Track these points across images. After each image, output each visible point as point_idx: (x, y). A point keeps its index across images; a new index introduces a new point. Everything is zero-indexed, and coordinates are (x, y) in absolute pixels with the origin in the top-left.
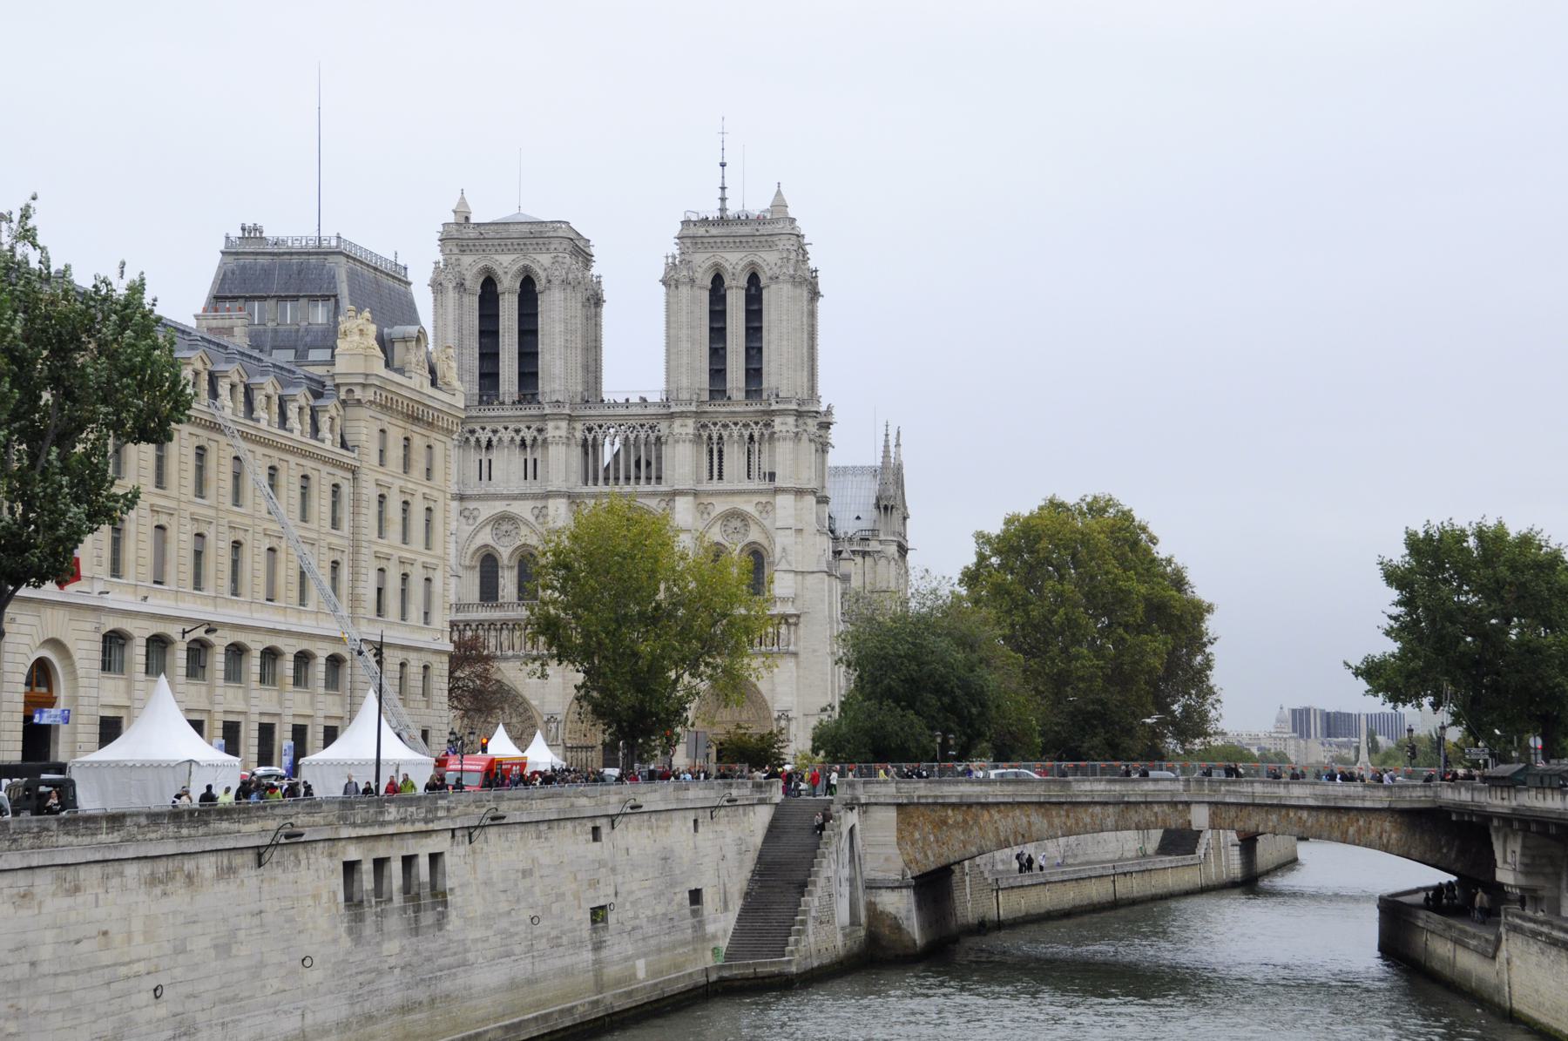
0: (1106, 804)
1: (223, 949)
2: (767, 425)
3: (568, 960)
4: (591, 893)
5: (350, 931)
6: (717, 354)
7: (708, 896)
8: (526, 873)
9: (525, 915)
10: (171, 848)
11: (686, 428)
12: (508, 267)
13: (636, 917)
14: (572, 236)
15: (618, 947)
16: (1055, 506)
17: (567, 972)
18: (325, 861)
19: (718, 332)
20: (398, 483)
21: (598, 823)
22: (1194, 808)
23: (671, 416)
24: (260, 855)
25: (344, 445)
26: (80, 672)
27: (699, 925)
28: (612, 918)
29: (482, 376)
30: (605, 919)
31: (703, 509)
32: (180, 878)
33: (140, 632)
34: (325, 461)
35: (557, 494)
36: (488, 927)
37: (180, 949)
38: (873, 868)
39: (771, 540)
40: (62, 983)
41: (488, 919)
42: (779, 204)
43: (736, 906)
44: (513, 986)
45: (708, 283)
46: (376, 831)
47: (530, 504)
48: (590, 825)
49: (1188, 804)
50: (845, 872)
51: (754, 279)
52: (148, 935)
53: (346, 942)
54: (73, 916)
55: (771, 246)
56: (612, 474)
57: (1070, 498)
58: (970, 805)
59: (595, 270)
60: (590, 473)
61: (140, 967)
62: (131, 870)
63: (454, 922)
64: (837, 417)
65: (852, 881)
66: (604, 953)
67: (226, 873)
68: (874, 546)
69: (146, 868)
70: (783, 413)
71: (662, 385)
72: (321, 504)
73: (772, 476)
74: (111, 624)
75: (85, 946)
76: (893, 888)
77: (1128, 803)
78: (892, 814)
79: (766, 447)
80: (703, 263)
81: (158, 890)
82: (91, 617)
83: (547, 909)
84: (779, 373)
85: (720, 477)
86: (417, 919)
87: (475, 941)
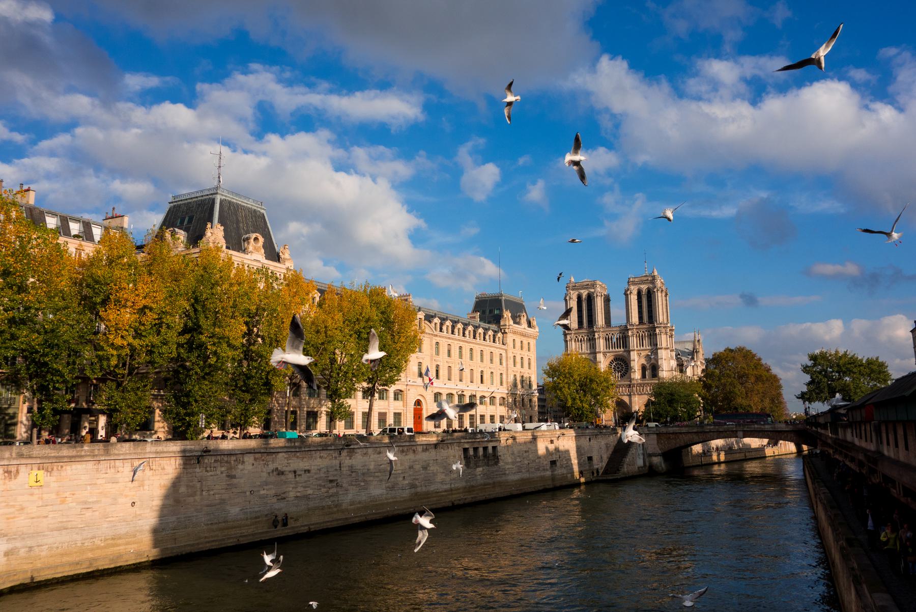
0: (714, 432)
1: (425, 468)
2: (655, 331)
3: (542, 474)
7: (595, 458)
8: (526, 452)
9: (526, 462)
12: (584, 293)
13: (567, 463)
14: (601, 283)
17: (542, 478)
18: (457, 448)
20: (526, 354)
21: (553, 439)
22: (738, 432)
25: (503, 344)
26: (428, 403)
28: (558, 464)
29: (578, 322)
31: (639, 355)
32: (411, 451)
33: (444, 393)
34: (497, 348)
35: (600, 352)
36: (513, 465)
37: (411, 467)
38: (650, 451)
39: (657, 362)
40: (376, 474)
41: (513, 463)
44: (522, 480)
46: (473, 440)
47: (592, 355)
48: (549, 439)
49: (737, 431)
54: (379, 459)
57: (733, 348)
58: (676, 433)
60: (607, 347)
61: (400, 472)
63: (501, 464)
65: (643, 454)
66: (556, 473)
70: (658, 327)
72: (496, 359)
73: (657, 345)
74: (436, 391)
75: (381, 466)
76: (656, 456)
77: (720, 431)
78: (655, 436)
79: (655, 337)
81: (404, 454)
83: (533, 461)
85: (643, 346)
86: (488, 463)
87: (508, 468)
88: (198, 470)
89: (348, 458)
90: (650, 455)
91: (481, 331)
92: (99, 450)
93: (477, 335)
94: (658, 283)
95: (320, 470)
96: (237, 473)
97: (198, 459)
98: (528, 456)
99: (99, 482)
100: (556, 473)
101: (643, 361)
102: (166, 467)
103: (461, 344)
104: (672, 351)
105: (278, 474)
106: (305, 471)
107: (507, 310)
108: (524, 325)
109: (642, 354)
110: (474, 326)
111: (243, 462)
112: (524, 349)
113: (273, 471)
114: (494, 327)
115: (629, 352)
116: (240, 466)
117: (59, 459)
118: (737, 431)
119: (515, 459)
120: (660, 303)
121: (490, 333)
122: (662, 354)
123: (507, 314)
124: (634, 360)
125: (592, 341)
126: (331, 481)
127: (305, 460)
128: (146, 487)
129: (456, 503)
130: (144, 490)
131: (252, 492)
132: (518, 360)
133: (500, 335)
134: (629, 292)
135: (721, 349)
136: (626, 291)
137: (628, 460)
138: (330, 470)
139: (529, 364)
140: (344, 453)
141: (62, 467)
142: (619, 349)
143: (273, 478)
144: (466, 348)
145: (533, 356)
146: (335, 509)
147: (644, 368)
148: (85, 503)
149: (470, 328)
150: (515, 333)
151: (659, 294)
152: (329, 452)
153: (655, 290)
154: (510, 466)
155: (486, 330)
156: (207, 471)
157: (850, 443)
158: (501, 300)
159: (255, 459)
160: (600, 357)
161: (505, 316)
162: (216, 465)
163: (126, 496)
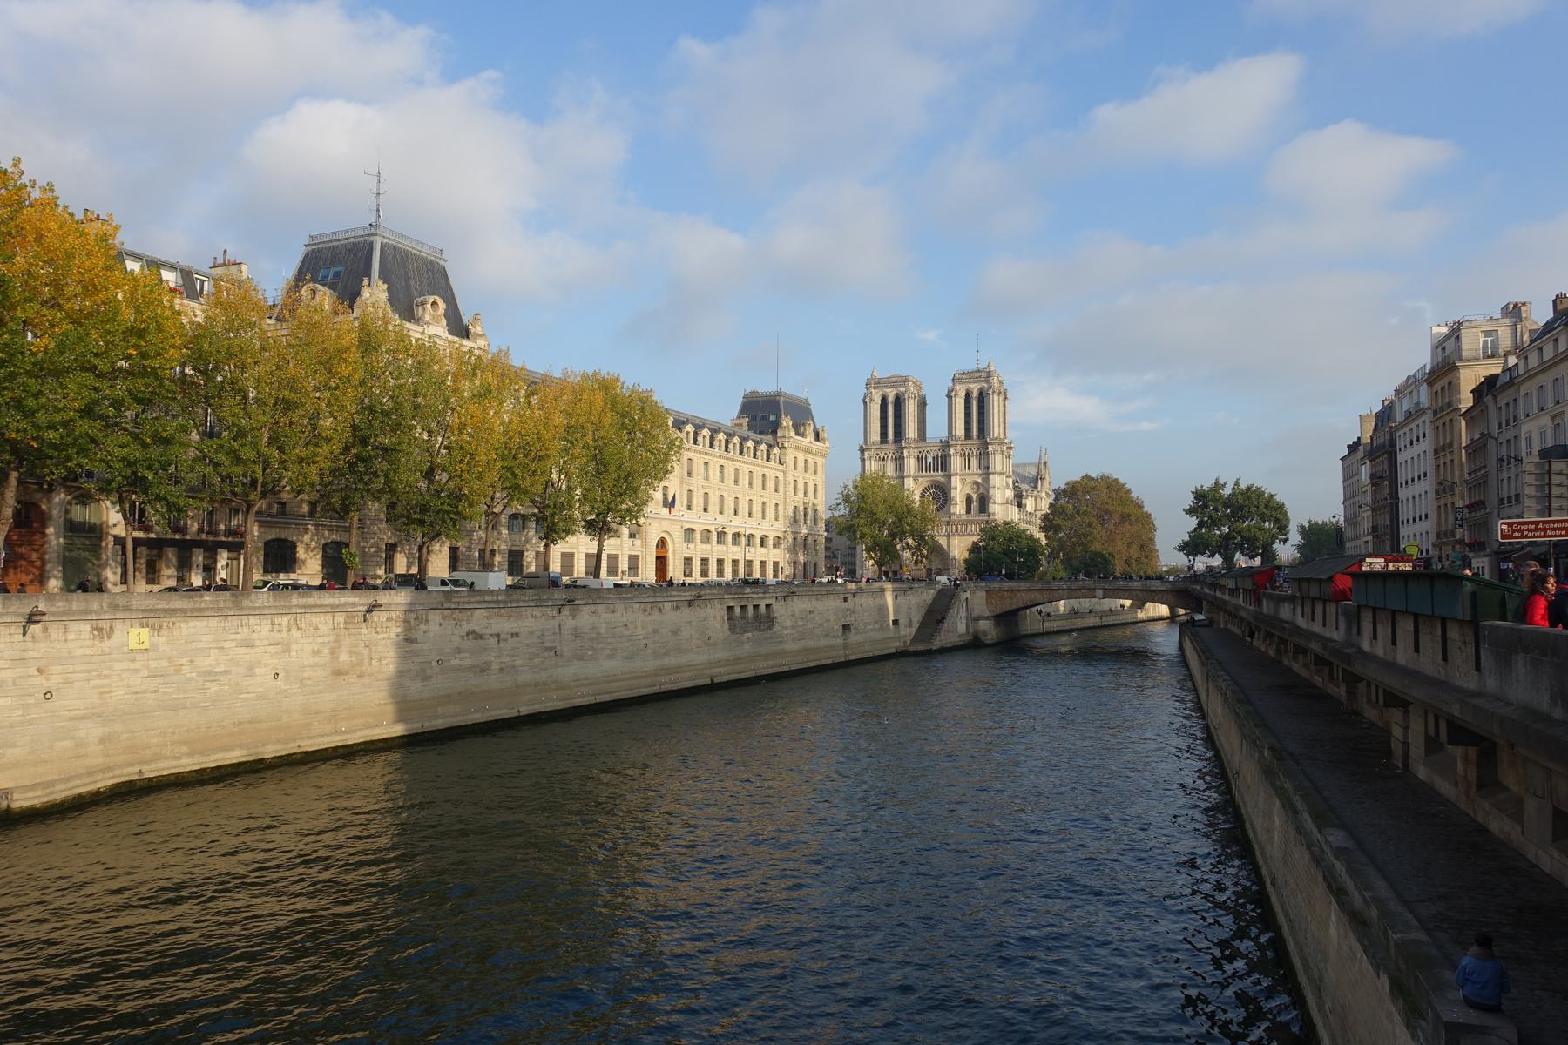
4: (843, 620)
5: (730, 629)
8: (810, 612)
9: (811, 626)
15: (853, 638)
16: (1087, 477)
23: (949, 446)
24: (690, 603)
25: (780, 463)
30: (849, 629)
31: (963, 481)
32: (657, 610)
33: (698, 528)
34: (772, 469)
35: (909, 476)
37: (656, 632)
38: (976, 613)
40: (609, 640)
41: (793, 627)
43: (916, 625)
45: (964, 394)
48: (842, 596)
50: (965, 614)
52: (643, 627)
53: (729, 633)
56: (928, 469)
57: (1094, 475)
62: (637, 605)
63: (777, 628)
65: (967, 618)
68: (1035, 492)
70: (991, 444)
71: (946, 434)
72: (771, 485)
73: (988, 468)
78: (984, 593)
82: (680, 524)
88: (364, 631)
89: (571, 617)
90: (977, 619)
91: (750, 444)
92: (225, 601)
93: (745, 450)
94: (995, 381)
95: (532, 633)
96: (418, 635)
98: (814, 618)
99: (226, 645)
100: (849, 641)
101: (968, 490)
102: (320, 626)
103: (723, 462)
104: (1008, 476)
106: (512, 634)
107: (786, 416)
108: (811, 438)
109: (968, 480)
110: (740, 437)
111: (427, 621)
112: (809, 472)
113: (468, 634)
114: (769, 438)
115: (949, 477)
116: (423, 627)
117: (170, 613)
118: (1095, 589)
119: (796, 622)
120: (996, 410)
121: (763, 447)
122: (996, 480)
123: (787, 422)
124: (956, 488)
125: (899, 460)
126: (550, 649)
127: (511, 619)
128: (294, 654)
129: (717, 680)
130: (290, 657)
132: (801, 486)
133: (776, 450)
134: (953, 394)
135: (1077, 477)
136: (950, 392)
137: (946, 625)
138: (546, 633)
139: (815, 491)
140: (566, 612)
141: (174, 623)
143: (469, 643)
144: (729, 468)
145: (819, 479)
146: (553, 686)
147: (969, 500)
148: (210, 673)
149: (736, 440)
150: (797, 448)
151: (996, 398)
152: (545, 609)
153: (990, 392)
154: (789, 632)
155: (757, 443)
156: (377, 633)
157: (1287, 622)
158: (778, 402)
160: (909, 483)
161: (784, 424)
162: (389, 624)
163: (266, 665)
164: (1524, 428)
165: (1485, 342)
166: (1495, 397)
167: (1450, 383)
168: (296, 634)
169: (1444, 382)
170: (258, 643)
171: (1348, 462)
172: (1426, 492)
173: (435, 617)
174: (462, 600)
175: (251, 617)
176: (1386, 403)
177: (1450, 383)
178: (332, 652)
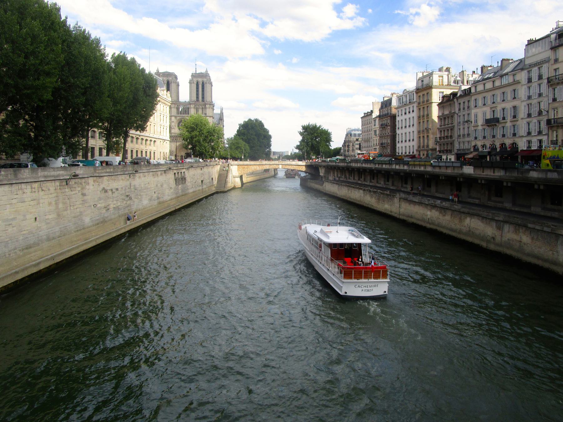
2: (205, 106)
6: (197, 94)
7: (214, 179)
8: (194, 175)
10: (155, 170)
11: (192, 106)
16: (250, 120)
19: (197, 91)
23: (190, 104)
27: (213, 183)
35: (173, 116)
41: (191, 182)
42: (207, 71)
45: (196, 83)
51: (203, 83)
53: (175, 185)
55: (206, 78)
56: (181, 113)
59: (178, 81)
62: (151, 173)
64: (215, 105)
67: (161, 174)
69: (153, 173)
70: (208, 104)
75: (147, 185)
80: (195, 80)
84: (207, 99)
88: (67, 190)
96: (85, 191)
97: (67, 181)
99: (14, 201)
105: (105, 192)
111: (88, 183)
116: (87, 187)
126: (127, 196)
127: (116, 181)
128: (41, 205)
131: (95, 206)
142: (184, 115)
143: (103, 195)
156: (71, 191)
159: (94, 181)
164: (473, 111)
165: (439, 80)
166: (457, 99)
167: (427, 93)
168: (42, 193)
169: (425, 92)
170: (26, 200)
171: (365, 119)
172: (413, 132)
173: (91, 180)
174: (100, 171)
175: (23, 184)
176: (386, 99)
177: (427, 93)
178: (56, 204)
